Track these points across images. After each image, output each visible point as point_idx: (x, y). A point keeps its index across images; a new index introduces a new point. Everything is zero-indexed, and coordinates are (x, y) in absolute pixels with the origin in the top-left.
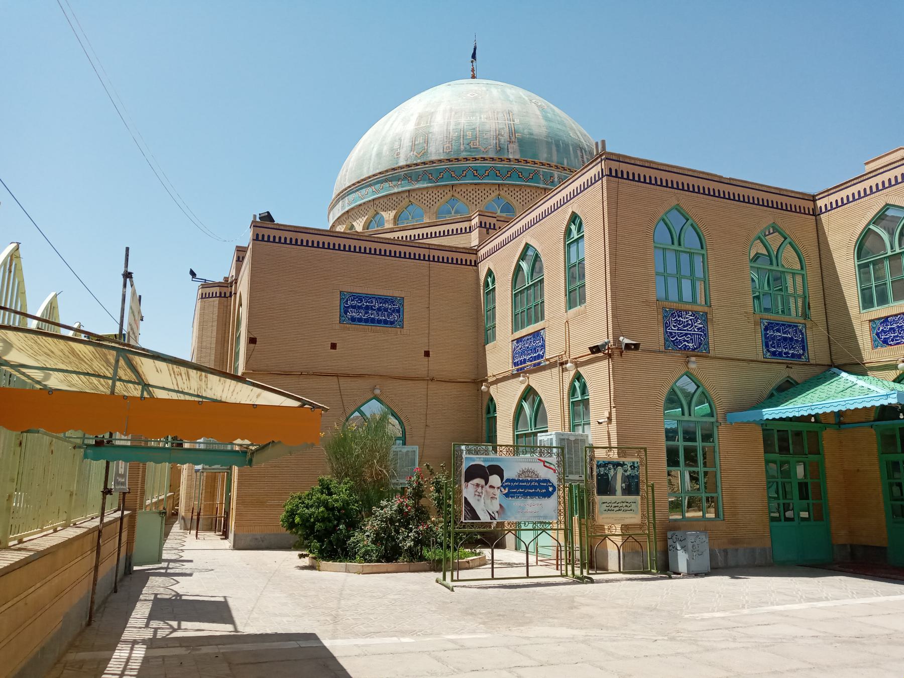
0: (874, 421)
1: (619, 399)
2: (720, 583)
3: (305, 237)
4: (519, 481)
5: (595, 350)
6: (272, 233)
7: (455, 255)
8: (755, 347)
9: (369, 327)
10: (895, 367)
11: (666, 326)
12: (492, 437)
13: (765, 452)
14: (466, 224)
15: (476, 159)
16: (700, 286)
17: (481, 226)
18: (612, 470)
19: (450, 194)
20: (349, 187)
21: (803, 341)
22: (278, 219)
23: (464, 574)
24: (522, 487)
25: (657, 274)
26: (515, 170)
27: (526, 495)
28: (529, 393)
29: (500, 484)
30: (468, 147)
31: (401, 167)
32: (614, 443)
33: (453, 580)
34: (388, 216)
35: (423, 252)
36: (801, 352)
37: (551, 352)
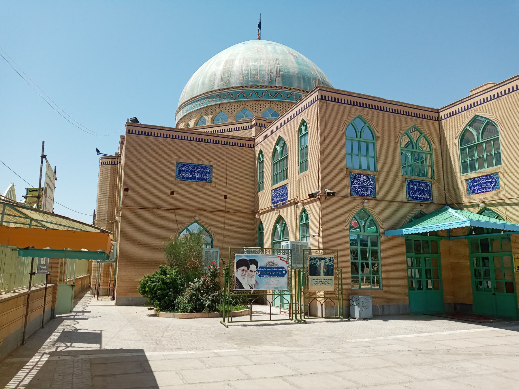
0: (468, 235)
1: (323, 223)
2: (377, 323)
3: (156, 131)
4: (267, 268)
5: (311, 196)
6: (138, 129)
7: (242, 142)
8: (402, 194)
10: (478, 206)
11: (352, 183)
12: (261, 244)
13: (407, 252)
14: (249, 124)
15: (257, 86)
16: (372, 160)
17: (257, 125)
18: (318, 262)
19: (243, 106)
20: (187, 101)
21: (430, 191)
22: (141, 122)
23: (234, 319)
24: (268, 271)
25: (348, 154)
27: (270, 275)
28: (280, 219)
29: (256, 270)
30: (253, 80)
31: (215, 91)
32: (321, 248)
33: (229, 322)
34: (208, 118)
35: (223, 140)
36: (429, 197)
37: (291, 197)
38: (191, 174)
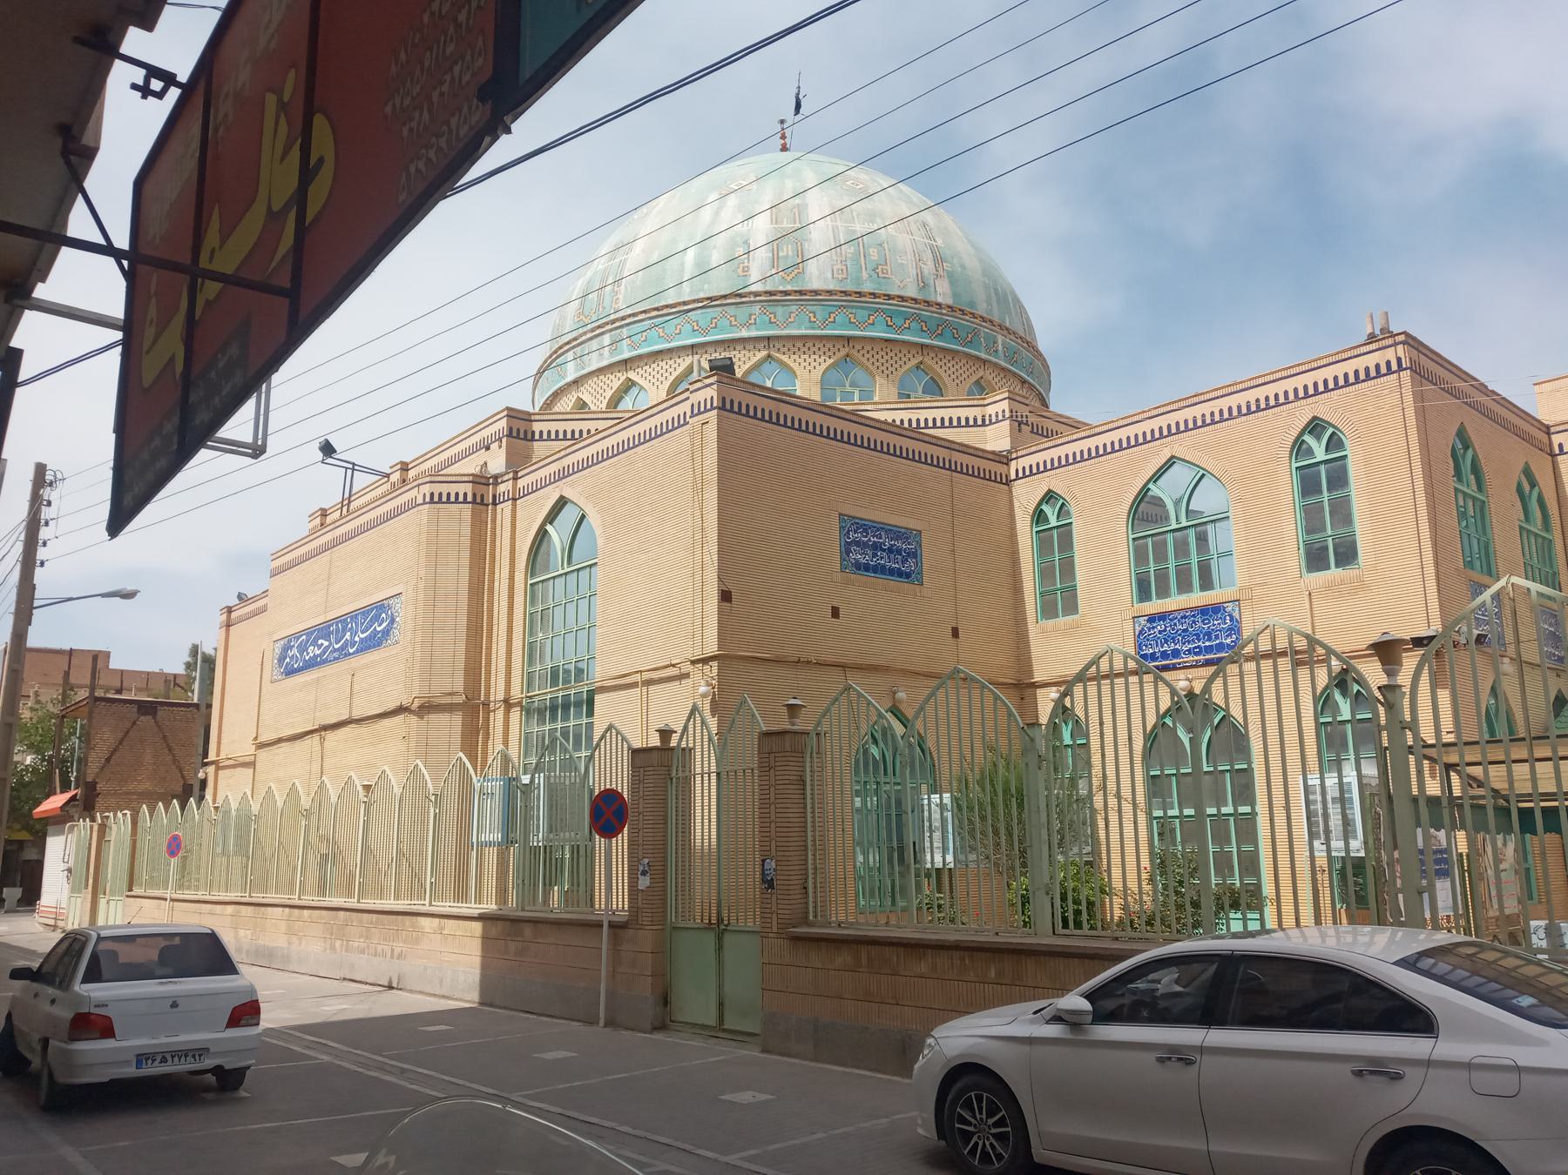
9: (880, 581)
15: (889, 297)
19: (843, 352)
26: (947, 324)
38: (875, 555)
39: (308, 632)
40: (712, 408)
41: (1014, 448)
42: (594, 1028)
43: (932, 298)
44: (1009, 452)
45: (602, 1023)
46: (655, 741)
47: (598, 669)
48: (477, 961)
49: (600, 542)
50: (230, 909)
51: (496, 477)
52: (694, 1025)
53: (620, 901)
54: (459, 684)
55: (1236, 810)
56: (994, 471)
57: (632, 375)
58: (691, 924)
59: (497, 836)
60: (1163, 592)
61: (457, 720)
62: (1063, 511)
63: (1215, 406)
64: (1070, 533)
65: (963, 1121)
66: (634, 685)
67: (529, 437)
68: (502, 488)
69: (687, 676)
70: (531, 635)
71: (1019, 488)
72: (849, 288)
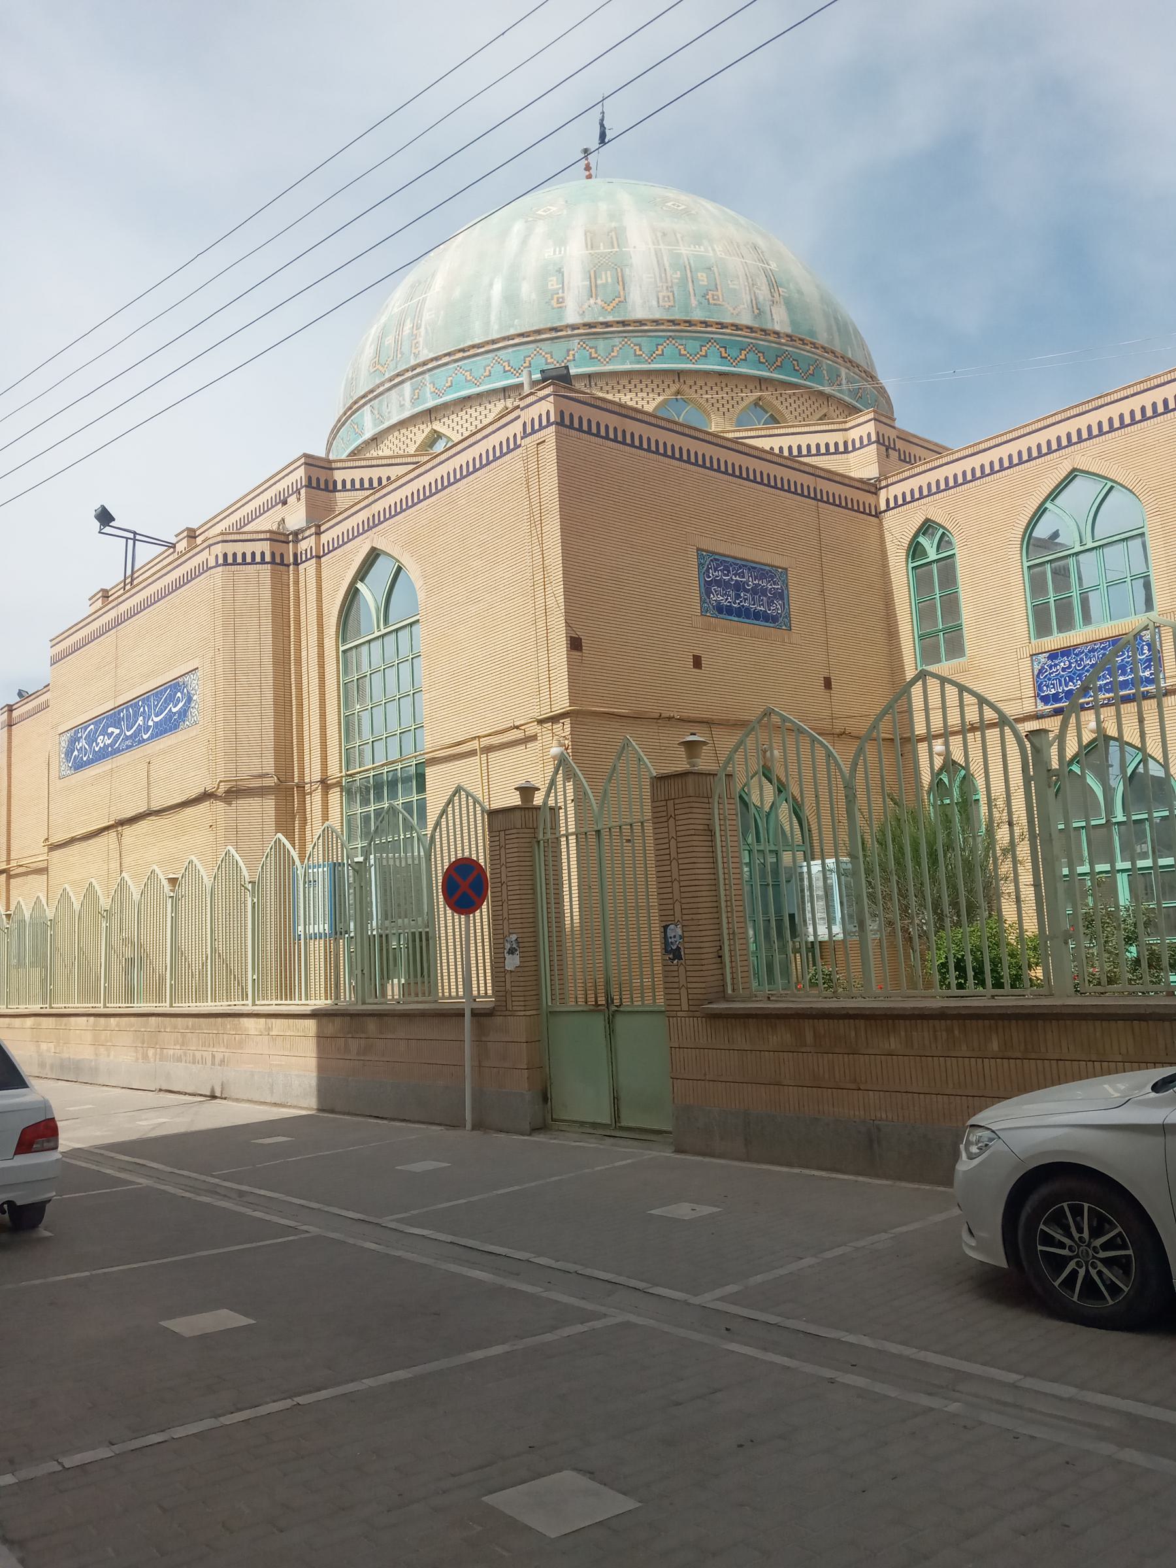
15: (723, 326)
17: (878, 442)
19: (674, 388)
39: (97, 720)
40: (549, 424)
41: (883, 475)
42: (453, 1133)
43: (769, 326)
44: (879, 480)
45: (469, 1125)
46: (515, 800)
47: (428, 739)
48: (312, 1063)
49: (421, 596)
50: (29, 1022)
51: (296, 534)
52: (582, 1124)
53: (483, 987)
54: (269, 766)
55: (1155, 862)
56: (861, 501)
57: (437, 426)
58: (571, 1005)
59: (322, 927)
60: (1066, 624)
61: (270, 803)
62: (944, 542)
63: (1124, 408)
64: (953, 568)
65: (1048, 1240)
66: (472, 753)
67: (330, 487)
68: (303, 545)
69: (533, 738)
70: (347, 707)
71: (891, 521)
72: (677, 316)
